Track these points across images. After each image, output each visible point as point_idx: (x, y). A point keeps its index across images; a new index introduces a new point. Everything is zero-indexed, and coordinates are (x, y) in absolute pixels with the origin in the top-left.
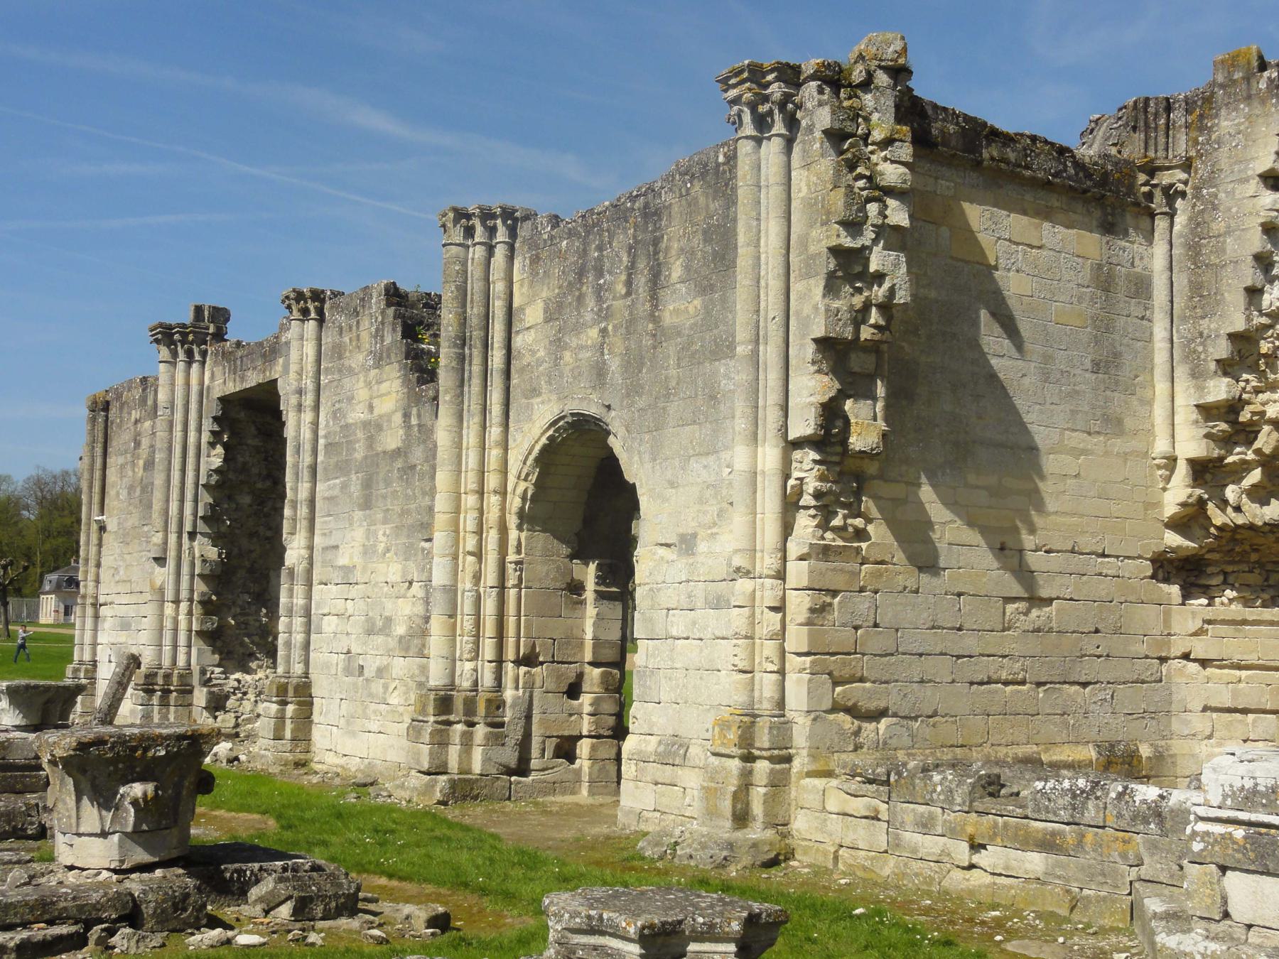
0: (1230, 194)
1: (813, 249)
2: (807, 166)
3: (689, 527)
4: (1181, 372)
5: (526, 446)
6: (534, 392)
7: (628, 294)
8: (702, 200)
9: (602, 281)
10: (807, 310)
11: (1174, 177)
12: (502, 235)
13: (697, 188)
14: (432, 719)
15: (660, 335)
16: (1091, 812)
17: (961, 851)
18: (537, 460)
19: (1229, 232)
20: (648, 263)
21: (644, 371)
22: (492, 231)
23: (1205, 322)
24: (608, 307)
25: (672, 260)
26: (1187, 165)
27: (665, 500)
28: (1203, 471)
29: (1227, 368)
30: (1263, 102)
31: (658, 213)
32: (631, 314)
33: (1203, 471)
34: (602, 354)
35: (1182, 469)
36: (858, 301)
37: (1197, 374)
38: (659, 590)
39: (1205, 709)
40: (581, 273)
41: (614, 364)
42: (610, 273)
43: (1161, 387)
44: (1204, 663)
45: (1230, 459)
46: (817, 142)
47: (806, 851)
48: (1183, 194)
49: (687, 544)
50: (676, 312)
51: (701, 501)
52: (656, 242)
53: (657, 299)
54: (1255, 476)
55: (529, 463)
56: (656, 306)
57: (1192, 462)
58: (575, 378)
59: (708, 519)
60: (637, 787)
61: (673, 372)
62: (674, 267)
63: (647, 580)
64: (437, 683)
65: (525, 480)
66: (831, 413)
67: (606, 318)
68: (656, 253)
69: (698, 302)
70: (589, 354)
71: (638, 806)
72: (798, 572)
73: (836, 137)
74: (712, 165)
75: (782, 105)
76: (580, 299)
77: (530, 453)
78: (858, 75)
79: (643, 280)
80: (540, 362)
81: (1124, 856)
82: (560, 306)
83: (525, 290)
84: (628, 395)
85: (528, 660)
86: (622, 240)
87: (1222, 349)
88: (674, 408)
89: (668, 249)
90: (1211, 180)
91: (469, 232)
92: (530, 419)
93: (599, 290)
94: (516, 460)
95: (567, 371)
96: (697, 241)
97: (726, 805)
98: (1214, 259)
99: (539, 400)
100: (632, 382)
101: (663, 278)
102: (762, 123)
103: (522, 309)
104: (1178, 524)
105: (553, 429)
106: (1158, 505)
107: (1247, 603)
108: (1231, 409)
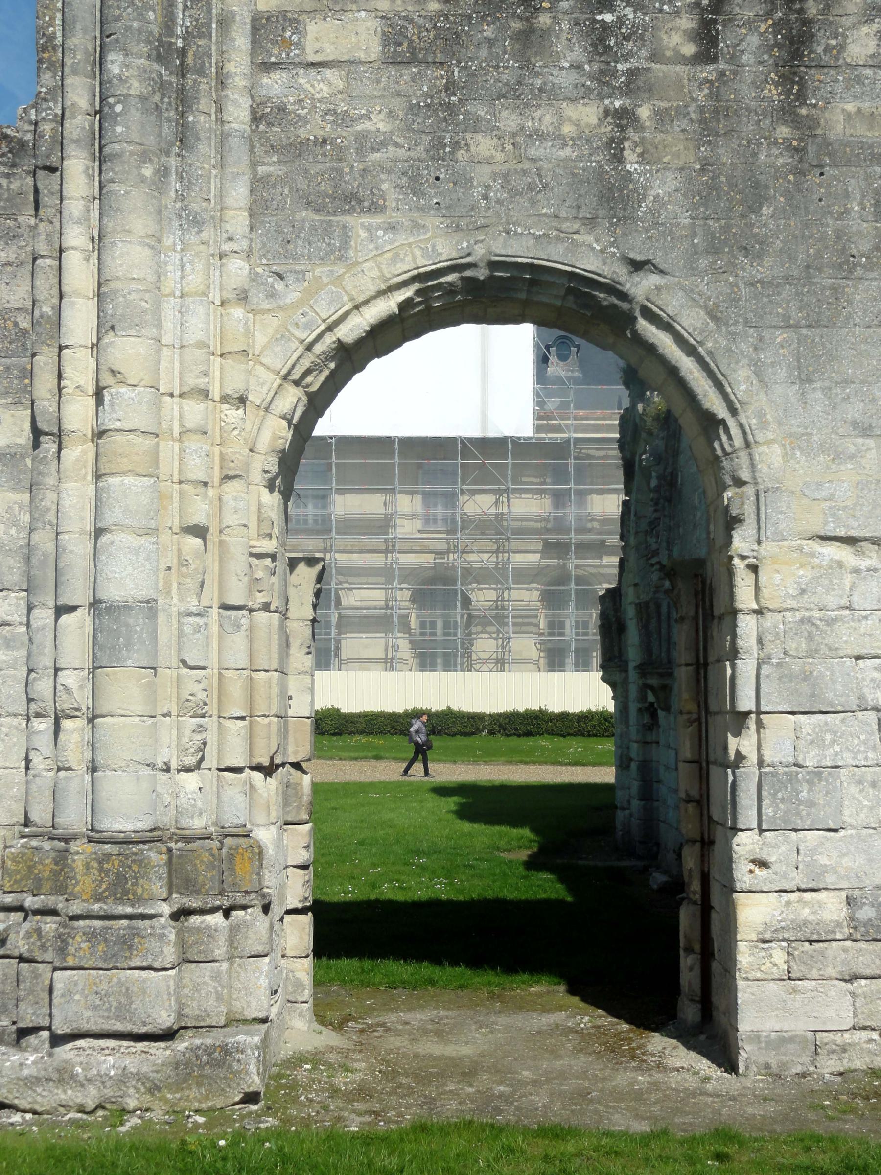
5: (326, 311)
9: (608, 17)
14: (166, 909)
20: (769, 14)
21: (765, 211)
24: (632, 73)
25: (847, 22)
27: (838, 457)
32: (715, 96)
34: (618, 158)
38: (830, 622)
53: (802, 84)
55: (319, 348)
56: (801, 97)
58: (514, 193)
60: (795, 991)
62: (852, 35)
63: (790, 603)
64: (140, 826)
65: (297, 383)
67: (628, 90)
70: (567, 152)
71: (800, 1026)
77: (330, 329)
79: (754, 40)
84: (713, 250)
94: (281, 337)
95: (482, 174)
99: (376, 220)
100: (726, 229)
101: (820, 49)
105: (416, 286)
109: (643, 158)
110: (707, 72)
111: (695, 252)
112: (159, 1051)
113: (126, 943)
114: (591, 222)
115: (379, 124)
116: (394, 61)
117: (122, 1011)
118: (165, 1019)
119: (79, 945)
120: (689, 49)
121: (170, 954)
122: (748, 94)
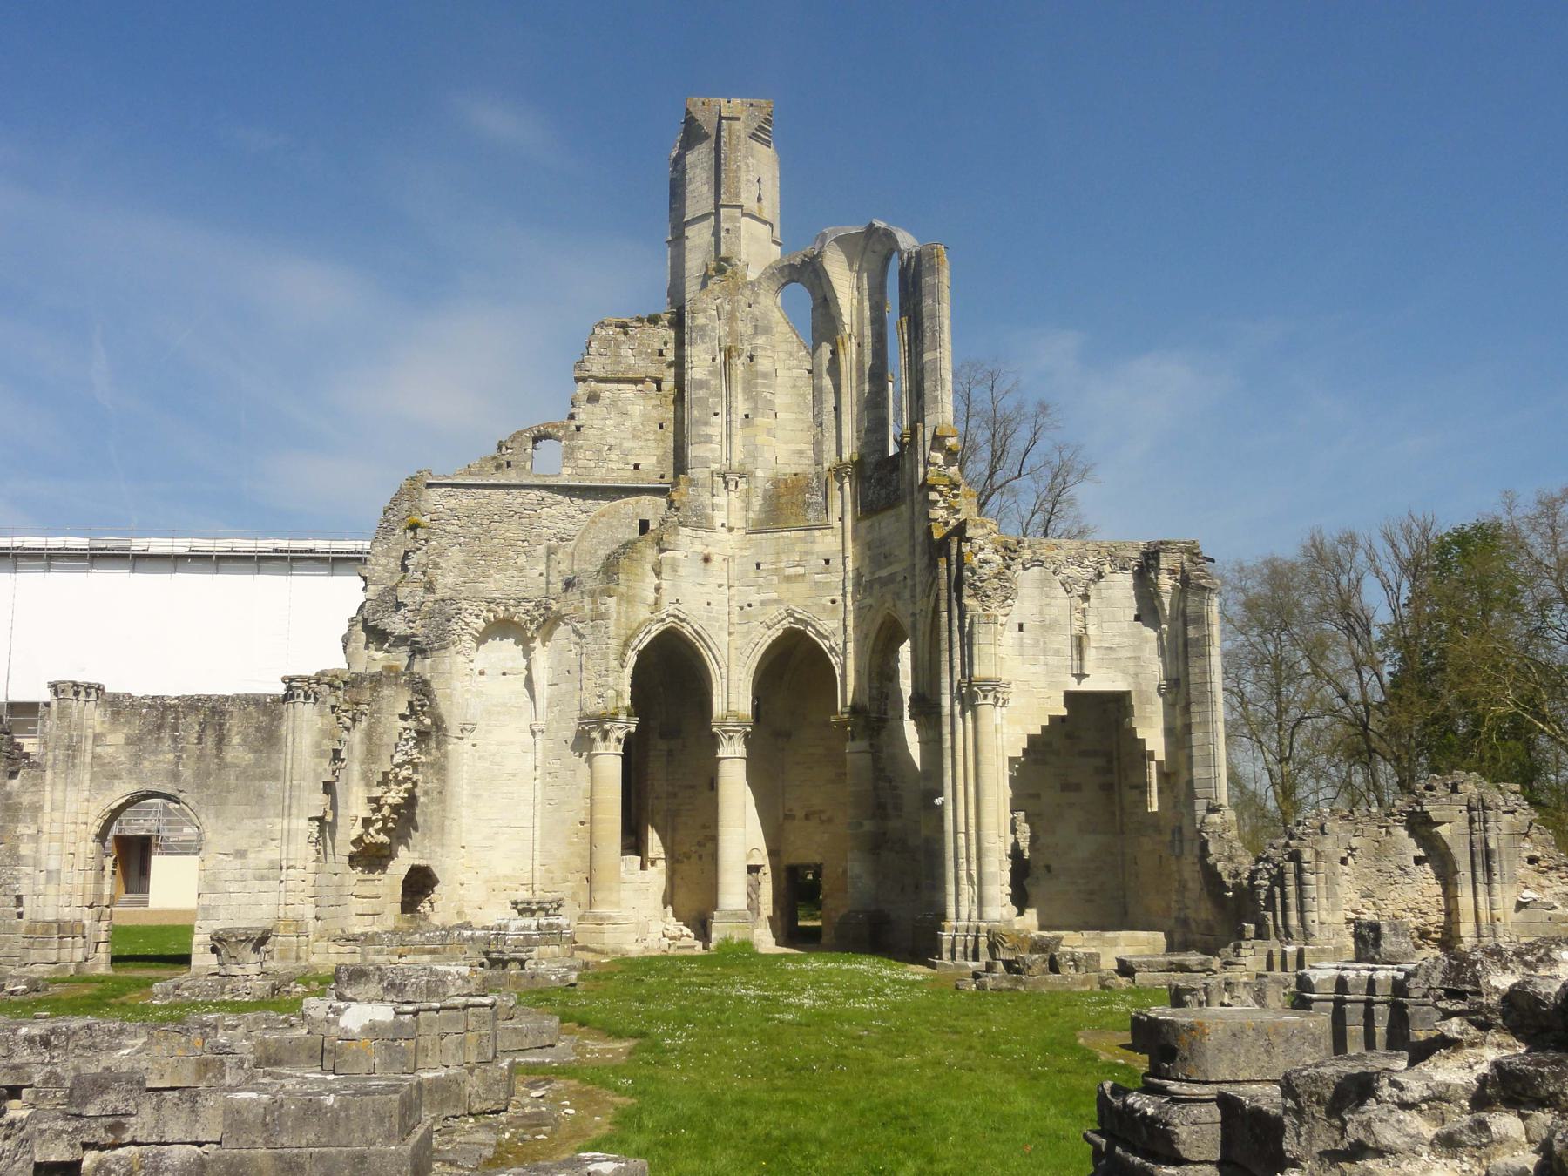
0: (387, 719)
1: (324, 748)
2: (322, 716)
3: (242, 845)
4: (363, 783)
6: (115, 777)
7: (199, 743)
8: (255, 714)
10: (320, 770)
11: (363, 707)
12: (93, 697)
13: (251, 709)
15: (222, 765)
16: (448, 941)
17: (395, 959)
18: (112, 811)
19: (385, 733)
22: (88, 694)
23: (373, 766)
26: (369, 705)
28: (367, 823)
29: (379, 784)
30: (402, 688)
31: (223, 713)
33: (367, 823)
34: (178, 766)
35: (360, 821)
36: (334, 767)
37: (368, 785)
39: (357, 914)
40: (159, 727)
41: (187, 773)
42: (184, 731)
43: (354, 789)
44: (356, 896)
45: (374, 818)
46: (329, 710)
47: (322, 968)
48: (366, 715)
49: (241, 854)
50: (237, 757)
51: (250, 837)
52: (221, 725)
54: (380, 824)
57: (364, 820)
59: (256, 844)
61: (232, 781)
66: (325, 812)
68: (221, 729)
69: (251, 756)
72: (312, 867)
73: (333, 707)
74: (262, 700)
75: (315, 693)
76: (159, 739)
78: (337, 683)
80: (119, 763)
81: (460, 952)
82: (140, 740)
83: (106, 725)
84: (198, 788)
85: (91, 906)
86: (193, 721)
87: (380, 777)
88: (232, 798)
89: (229, 730)
90: (378, 711)
91: (77, 693)
92: (111, 789)
93: (175, 740)
96: (252, 731)
97: (293, 954)
98: (378, 742)
102: (307, 697)
103: (104, 735)
104: (353, 843)
106: (349, 835)
107: (363, 872)
108: (376, 800)
109: (183, 767)
110: (200, 746)
111: (193, 789)
112: (53, 966)
113: (47, 944)
114: (171, 781)
115: (122, 759)
116: (127, 744)
117: (45, 958)
118: (54, 960)
119: (36, 944)
120: (196, 741)
121: (56, 946)
122: (209, 752)
